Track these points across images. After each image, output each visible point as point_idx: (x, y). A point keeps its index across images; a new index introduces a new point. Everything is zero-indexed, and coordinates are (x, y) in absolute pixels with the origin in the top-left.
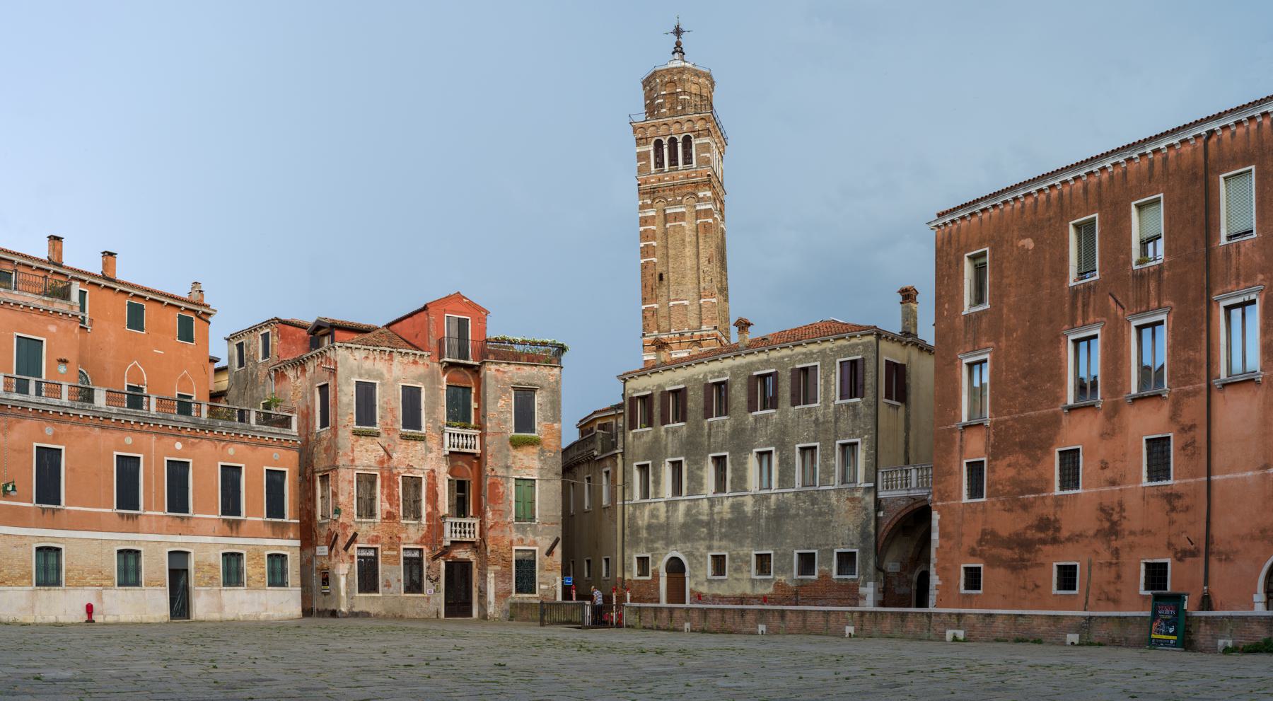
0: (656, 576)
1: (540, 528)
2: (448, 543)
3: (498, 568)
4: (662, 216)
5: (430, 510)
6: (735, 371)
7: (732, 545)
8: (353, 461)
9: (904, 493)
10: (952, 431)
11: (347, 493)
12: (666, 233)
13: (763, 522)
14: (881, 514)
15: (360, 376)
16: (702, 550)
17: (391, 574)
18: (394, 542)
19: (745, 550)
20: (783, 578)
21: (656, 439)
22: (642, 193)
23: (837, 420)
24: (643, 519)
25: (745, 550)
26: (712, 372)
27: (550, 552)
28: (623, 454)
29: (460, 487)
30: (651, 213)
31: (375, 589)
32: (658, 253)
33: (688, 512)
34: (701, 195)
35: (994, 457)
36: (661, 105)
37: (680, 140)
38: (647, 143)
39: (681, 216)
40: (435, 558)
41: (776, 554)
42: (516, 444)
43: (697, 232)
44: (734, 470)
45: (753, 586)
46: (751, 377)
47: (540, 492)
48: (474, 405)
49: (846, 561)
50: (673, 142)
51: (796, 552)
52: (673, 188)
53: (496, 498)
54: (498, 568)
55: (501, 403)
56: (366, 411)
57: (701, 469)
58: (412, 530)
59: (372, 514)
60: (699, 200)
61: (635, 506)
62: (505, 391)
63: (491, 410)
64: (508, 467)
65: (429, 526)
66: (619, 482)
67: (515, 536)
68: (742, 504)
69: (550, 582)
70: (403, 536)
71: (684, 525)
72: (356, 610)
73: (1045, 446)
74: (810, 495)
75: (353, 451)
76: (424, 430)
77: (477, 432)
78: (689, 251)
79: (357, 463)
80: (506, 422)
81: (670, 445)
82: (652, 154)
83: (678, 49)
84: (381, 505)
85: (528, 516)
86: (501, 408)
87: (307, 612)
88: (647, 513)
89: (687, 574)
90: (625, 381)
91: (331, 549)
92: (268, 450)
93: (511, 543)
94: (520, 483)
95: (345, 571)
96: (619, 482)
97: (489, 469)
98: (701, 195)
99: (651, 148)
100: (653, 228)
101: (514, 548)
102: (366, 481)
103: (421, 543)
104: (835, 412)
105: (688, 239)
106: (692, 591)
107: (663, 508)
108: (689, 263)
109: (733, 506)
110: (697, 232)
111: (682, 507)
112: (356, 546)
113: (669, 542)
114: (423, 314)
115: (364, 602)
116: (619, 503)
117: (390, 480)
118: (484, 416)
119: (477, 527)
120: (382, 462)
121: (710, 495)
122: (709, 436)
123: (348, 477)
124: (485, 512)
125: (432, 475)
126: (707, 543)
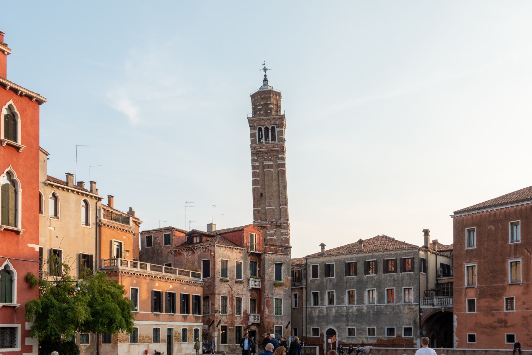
4: (262, 166)
6: (358, 259)
7: (358, 324)
10: (461, 289)
11: (218, 305)
12: (264, 174)
13: (371, 316)
14: (422, 314)
16: (344, 326)
17: (231, 335)
19: (364, 326)
20: (381, 337)
21: (322, 282)
22: (253, 154)
23: (403, 280)
24: (316, 313)
25: (364, 326)
26: (348, 259)
27: (287, 327)
28: (306, 288)
31: (226, 342)
32: (261, 183)
33: (337, 311)
34: (280, 156)
35: (479, 298)
36: (260, 110)
37: (270, 128)
38: (255, 129)
40: (245, 330)
41: (377, 328)
42: (275, 285)
44: (358, 296)
45: (367, 340)
46: (365, 262)
48: (258, 269)
50: (267, 129)
51: (386, 327)
52: (267, 152)
55: (270, 269)
56: (224, 272)
57: (343, 295)
58: (238, 318)
59: (225, 313)
62: (271, 264)
64: (273, 294)
66: (304, 298)
67: (275, 321)
68: (362, 309)
70: (235, 321)
71: (335, 316)
72: (220, 351)
73: (500, 296)
74: (392, 307)
76: (242, 279)
77: (260, 280)
78: (275, 183)
79: (221, 292)
80: (272, 276)
81: (328, 285)
82: (257, 134)
83: (265, 80)
84: (229, 309)
86: (270, 272)
88: (317, 311)
90: (307, 259)
92: (195, 287)
93: (274, 323)
95: (216, 335)
96: (304, 298)
98: (280, 156)
99: (257, 131)
100: (258, 171)
102: (224, 299)
104: (402, 277)
105: (274, 178)
107: (325, 310)
108: (275, 189)
109: (358, 310)
111: (334, 310)
112: (221, 325)
113: (328, 323)
114: (240, 232)
116: (304, 307)
117: (232, 299)
118: (264, 274)
120: (229, 292)
121: (347, 305)
122: (347, 283)
123: (218, 298)
126: (346, 323)
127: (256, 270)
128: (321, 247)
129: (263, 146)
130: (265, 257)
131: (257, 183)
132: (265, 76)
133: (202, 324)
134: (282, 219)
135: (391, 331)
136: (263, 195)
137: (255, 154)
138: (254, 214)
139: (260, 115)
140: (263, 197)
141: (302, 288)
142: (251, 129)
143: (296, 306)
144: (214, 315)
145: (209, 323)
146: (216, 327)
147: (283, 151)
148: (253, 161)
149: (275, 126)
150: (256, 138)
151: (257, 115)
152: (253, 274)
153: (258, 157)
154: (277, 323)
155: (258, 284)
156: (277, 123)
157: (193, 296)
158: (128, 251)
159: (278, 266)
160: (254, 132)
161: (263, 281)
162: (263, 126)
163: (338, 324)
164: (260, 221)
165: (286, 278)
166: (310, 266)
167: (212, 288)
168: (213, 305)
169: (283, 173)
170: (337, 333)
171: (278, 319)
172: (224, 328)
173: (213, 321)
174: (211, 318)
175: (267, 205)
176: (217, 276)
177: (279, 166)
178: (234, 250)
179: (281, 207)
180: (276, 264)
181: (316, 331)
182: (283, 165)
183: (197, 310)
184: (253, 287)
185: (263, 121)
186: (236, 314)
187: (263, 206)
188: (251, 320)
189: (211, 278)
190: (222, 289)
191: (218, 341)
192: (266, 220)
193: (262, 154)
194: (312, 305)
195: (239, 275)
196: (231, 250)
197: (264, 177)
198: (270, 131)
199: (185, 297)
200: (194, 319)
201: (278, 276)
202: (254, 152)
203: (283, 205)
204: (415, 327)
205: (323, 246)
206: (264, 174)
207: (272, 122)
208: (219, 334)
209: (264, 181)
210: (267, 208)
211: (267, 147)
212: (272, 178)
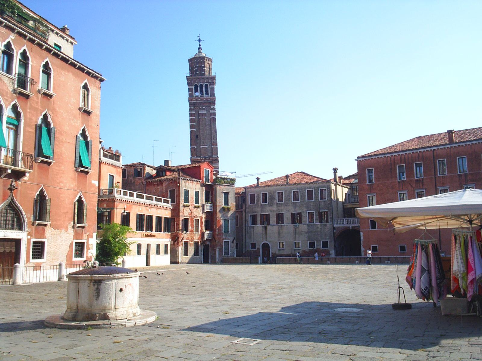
0: (258, 249)
3: (219, 247)
4: (197, 113)
8: (183, 214)
9: (343, 226)
15: (186, 188)
18: (192, 238)
22: (191, 104)
27: (233, 242)
30: (194, 112)
34: (212, 107)
37: (204, 85)
38: (192, 85)
48: (210, 196)
50: (201, 86)
52: (202, 103)
54: (219, 247)
56: (187, 200)
58: (196, 236)
60: (211, 109)
61: (250, 227)
63: (218, 198)
67: (224, 237)
70: (194, 237)
75: (184, 211)
78: (208, 127)
82: (194, 89)
84: (190, 228)
89: (270, 248)
96: (244, 219)
99: (193, 87)
100: (194, 118)
101: (224, 241)
103: (198, 240)
105: (207, 123)
108: (207, 132)
112: (184, 241)
118: (216, 200)
120: (190, 214)
124: (215, 231)
127: (209, 197)
128: (257, 180)
129: (198, 99)
130: (216, 188)
134: (213, 156)
135: (312, 245)
136: (198, 136)
137: (192, 104)
138: (191, 151)
139: (196, 75)
140: (198, 139)
141: (242, 212)
142: (188, 85)
144: (179, 233)
145: (175, 239)
146: (180, 242)
147: (214, 103)
148: (190, 110)
150: (193, 92)
151: (193, 75)
152: (207, 200)
153: (194, 108)
154: (225, 238)
156: (210, 81)
157: (164, 218)
158: (118, 182)
159: (226, 194)
160: (191, 87)
162: (198, 83)
164: (195, 157)
165: (232, 203)
166: (248, 194)
167: (177, 211)
169: (214, 120)
170: (270, 246)
171: (226, 236)
172: (186, 244)
173: (178, 238)
175: (202, 144)
176: (181, 202)
178: (195, 182)
179: (213, 147)
181: (253, 245)
183: (167, 230)
185: (198, 80)
187: (198, 145)
189: (176, 203)
190: (185, 213)
192: (200, 157)
193: (198, 105)
195: (197, 201)
196: (191, 182)
197: (199, 122)
198: (204, 87)
199: (159, 219)
201: (226, 203)
204: (331, 242)
205: (258, 179)
207: (206, 81)
209: (199, 125)
210: (201, 147)
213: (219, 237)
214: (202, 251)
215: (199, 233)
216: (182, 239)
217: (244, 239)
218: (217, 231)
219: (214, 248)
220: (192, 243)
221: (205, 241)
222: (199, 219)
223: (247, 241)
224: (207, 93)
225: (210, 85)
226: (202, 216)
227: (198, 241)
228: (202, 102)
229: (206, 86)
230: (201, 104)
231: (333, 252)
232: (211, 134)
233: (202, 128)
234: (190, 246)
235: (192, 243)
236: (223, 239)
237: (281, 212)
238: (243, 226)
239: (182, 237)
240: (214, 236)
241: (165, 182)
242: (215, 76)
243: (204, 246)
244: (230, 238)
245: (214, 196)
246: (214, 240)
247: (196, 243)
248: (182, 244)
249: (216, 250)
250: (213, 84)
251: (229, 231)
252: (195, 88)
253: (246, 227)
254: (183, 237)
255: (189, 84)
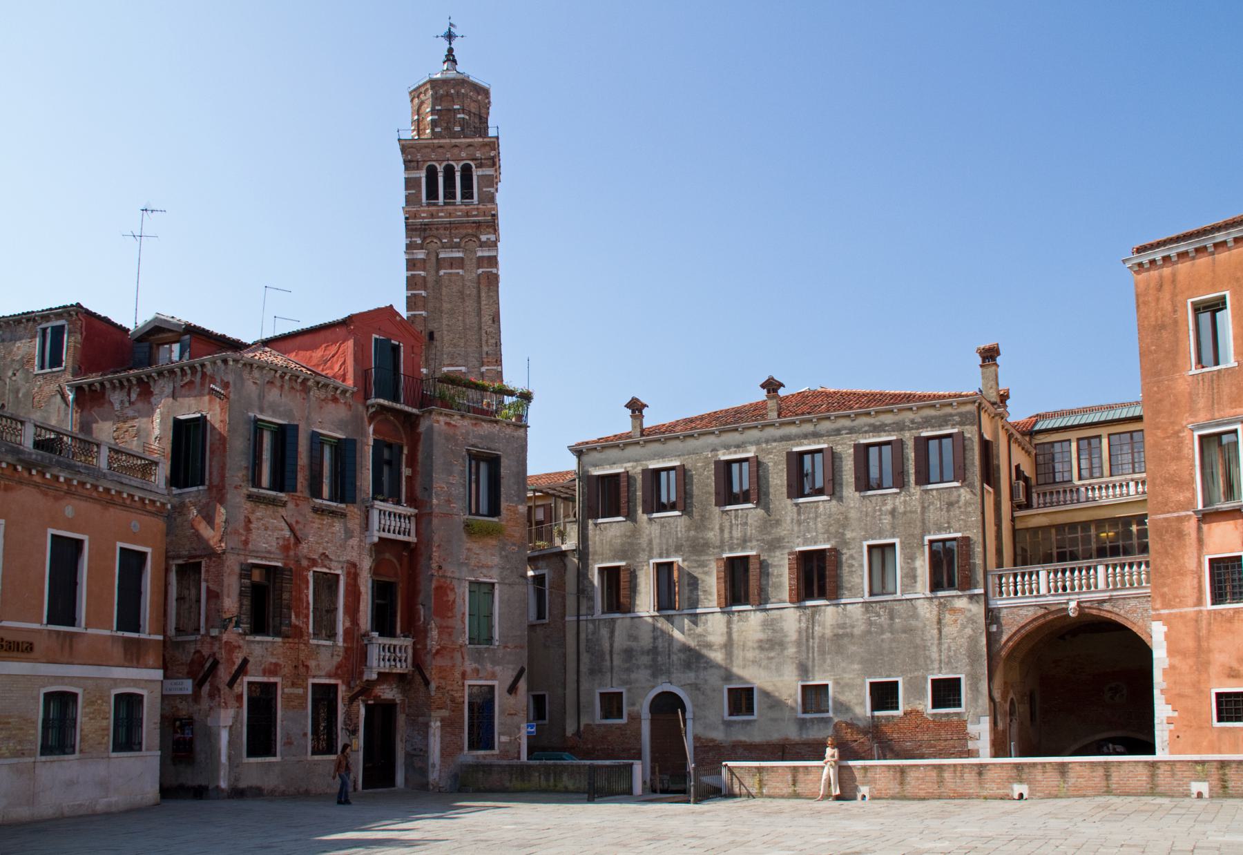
1: (500, 653)
2: (374, 676)
3: (445, 713)
4: (433, 259)
5: (348, 624)
8: (246, 542)
18: (300, 670)
22: (410, 229)
27: (512, 689)
29: (383, 590)
30: (420, 255)
31: (269, 750)
37: (458, 168)
38: (418, 168)
39: (460, 263)
40: (352, 699)
43: (479, 283)
47: (501, 602)
48: (406, 471)
49: (946, 692)
52: (451, 227)
53: (444, 608)
54: (445, 713)
60: (482, 245)
65: (347, 650)
67: (469, 665)
69: (514, 729)
70: (312, 664)
72: (242, 785)
75: (248, 530)
77: (411, 511)
78: (470, 305)
81: (656, 542)
82: (424, 181)
83: (450, 58)
85: (484, 636)
87: (168, 791)
91: (198, 685)
94: (475, 588)
95: (227, 723)
97: (434, 565)
98: (483, 238)
99: (423, 174)
100: (422, 273)
101: (468, 682)
106: (697, 738)
110: (479, 283)
112: (246, 679)
113: (657, 671)
115: (255, 771)
116: (570, 618)
118: (428, 489)
119: (410, 651)
120: (286, 548)
124: (425, 632)
125: (353, 575)
129: (438, 212)
130: (431, 428)
131: (420, 303)
132: (450, 51)
133: (158, 674)
136: (436, 335)
137: (416, 230)
142: (407, 169)
143: (540, 615)
146: (225, 690)
147: (492, 224)
148: (410, 247)
149: (472, 163)
150: (420, 191)
153: (424, 239)
154: (477, 671)
155: (404, 524)
156: (478, 155)
160: (414, 174)
161: (422, 519)
163: (691, 676)
168: (214, 596)
169: (493, 280)
173: (216, 664)
174: (206, 651)
177: (481, 261)
179: (483, 369)
180: (475, 458)
181: (612, 704)
182: (493, 261)
184: (385, 535)
186: (316, 635)
188: (376, 663)
191: (231, 743)
193: (435, 232)
194: (598, 613)
200: (118, 652)
202: (413, 224)
203: (489, 363)
206: (438, 281)
208: (236, 718)
211: (450, 215)
212: (462, 293)
213: (439, 661)
214: (354, 732)
215: (340, 641)
216: (243, 669)
217: (571, 677)
218: (435, 633)
219: (421, 719)
220: (300, 691)
221: (370, 684)
222: (338, 576)
223: (585, 685)
224: (467, 194)
225: (480, 166)
226: (355, 559)
227: (332, 681)
228: (450, 223)
229: (467, 172)
230: (445, 229)
231: (981, 731)
232: (480, 328)
233: (449, 306)
234: (285, 708)
235: (300, 691)
236: (464, 676)
237: (744, 549)
238: (567, 618)
239: (238, 661)
240: (418, 665)
241: (161, 382)
242: (497, 138)
243: (368, 707)
244: (498, 669)
245: (419, 468)
246: (418, 679)
247: (325, 696)
248: (239, 698)
249: (427, 725)
250: (494, 162)
251: (496, 636)
252: (427, 177)
253: (578, 621)
254: (245, 661)
255: (408, 164)
